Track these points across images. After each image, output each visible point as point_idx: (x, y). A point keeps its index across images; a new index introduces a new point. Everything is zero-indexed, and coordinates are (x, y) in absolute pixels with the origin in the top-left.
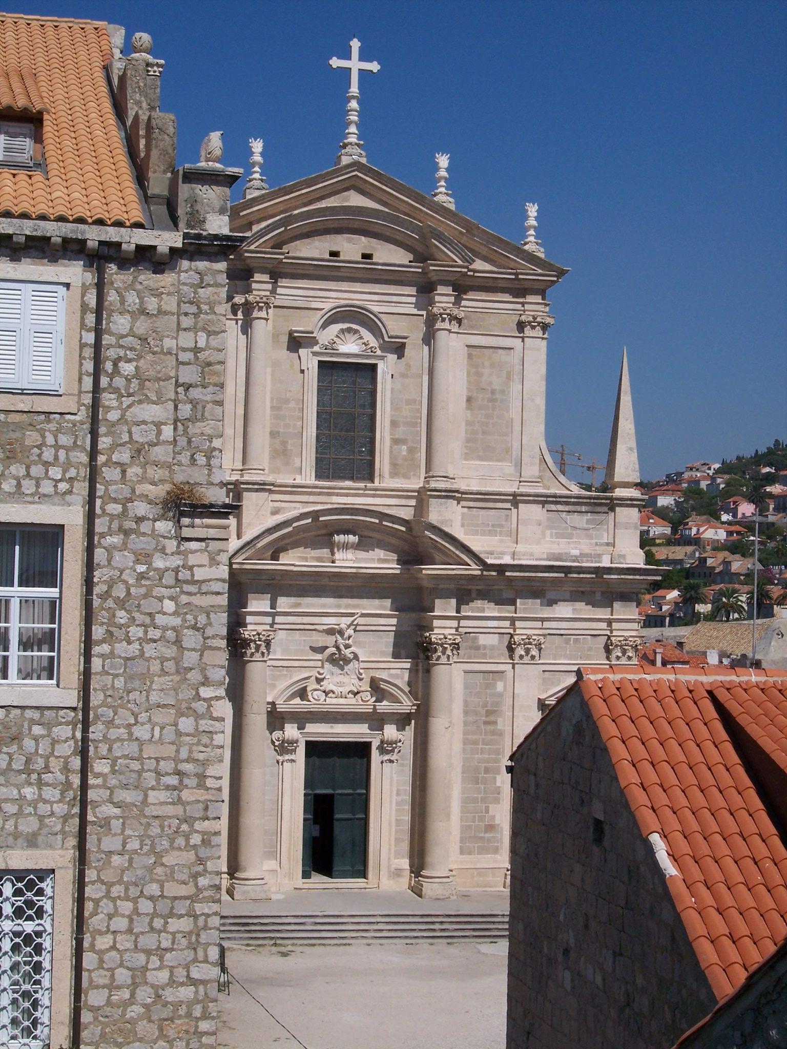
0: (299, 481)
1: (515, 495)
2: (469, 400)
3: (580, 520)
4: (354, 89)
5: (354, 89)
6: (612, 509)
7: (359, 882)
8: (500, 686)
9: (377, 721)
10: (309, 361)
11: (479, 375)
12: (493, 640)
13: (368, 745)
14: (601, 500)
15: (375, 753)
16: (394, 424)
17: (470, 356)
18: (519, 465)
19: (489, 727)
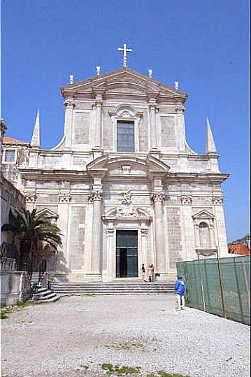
0: (112, 152)
1: (178, 155)
2: (162, 131)
3: (199, 163)
4: (125, 55)
5: (125, 55)
6: (209, 159)
7: (136, 278)
8: (179, 213)
9: (139, 222)
10: (114, 119)
11: (165, 124)
12: (175, 198)
13: (136, 232)
14: (206, 157)
15: (139, 233)
16: (140, 137)
17: (162, 119)
18: (178, 148)
19: (177, 226)
